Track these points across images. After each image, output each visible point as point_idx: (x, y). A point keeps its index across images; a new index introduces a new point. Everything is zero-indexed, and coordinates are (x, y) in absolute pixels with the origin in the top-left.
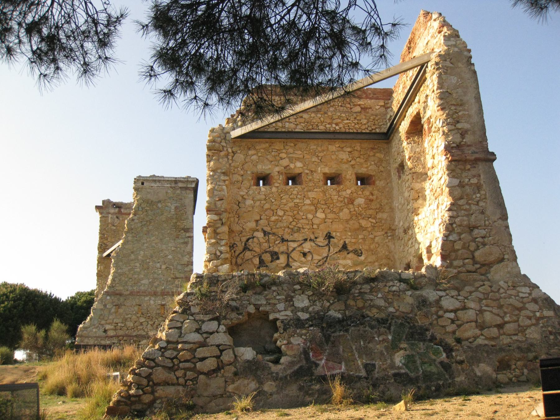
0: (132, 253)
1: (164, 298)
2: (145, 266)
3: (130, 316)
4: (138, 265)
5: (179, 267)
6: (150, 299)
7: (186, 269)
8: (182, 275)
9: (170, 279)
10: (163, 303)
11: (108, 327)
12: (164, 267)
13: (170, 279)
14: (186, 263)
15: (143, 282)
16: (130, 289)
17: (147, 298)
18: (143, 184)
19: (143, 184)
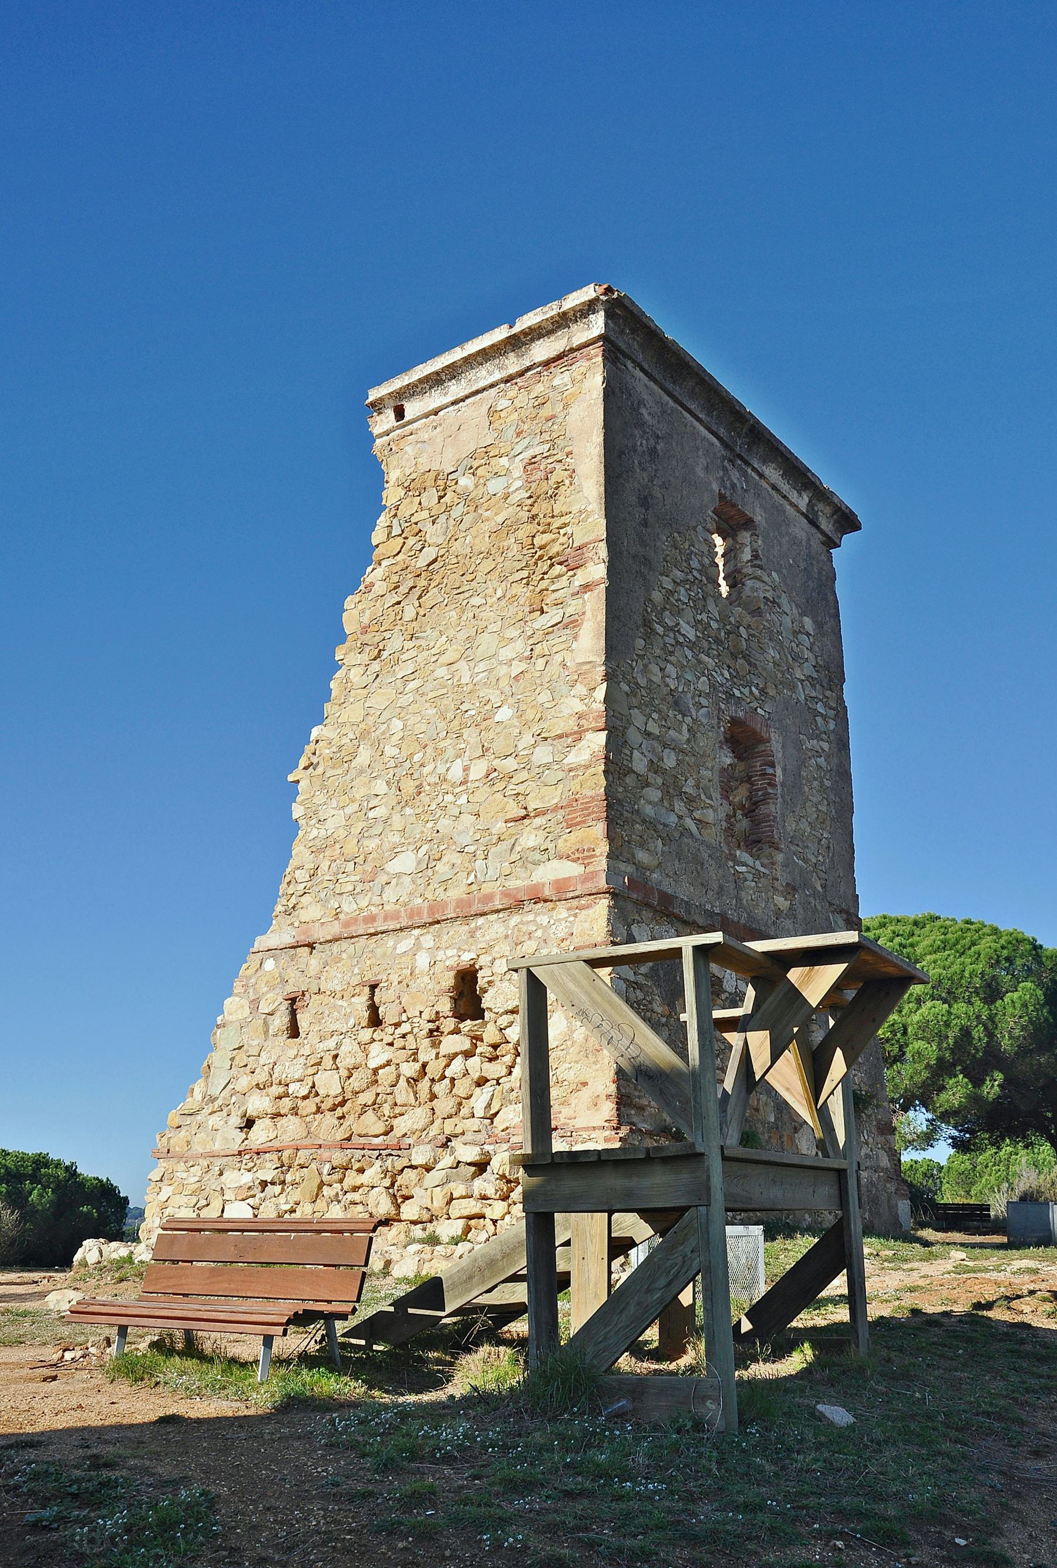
0: (364, 735)
1: (472, 934)
2: (409, 786)
3: (331, 1043)
4: (380, 787)
5: (543, 754)
6: (418, 946)
7: (572, 759)
8: (554, 797)
9: (499, 827)
10: (466, 957)
11: (258, 1103)
12: (478, 770)
13: (499, 827)
14: (572, 725)
15: (393, 867)
16: (348, 907)
17: (406, 943)
18: (400, 413)
19: (400, 413)
